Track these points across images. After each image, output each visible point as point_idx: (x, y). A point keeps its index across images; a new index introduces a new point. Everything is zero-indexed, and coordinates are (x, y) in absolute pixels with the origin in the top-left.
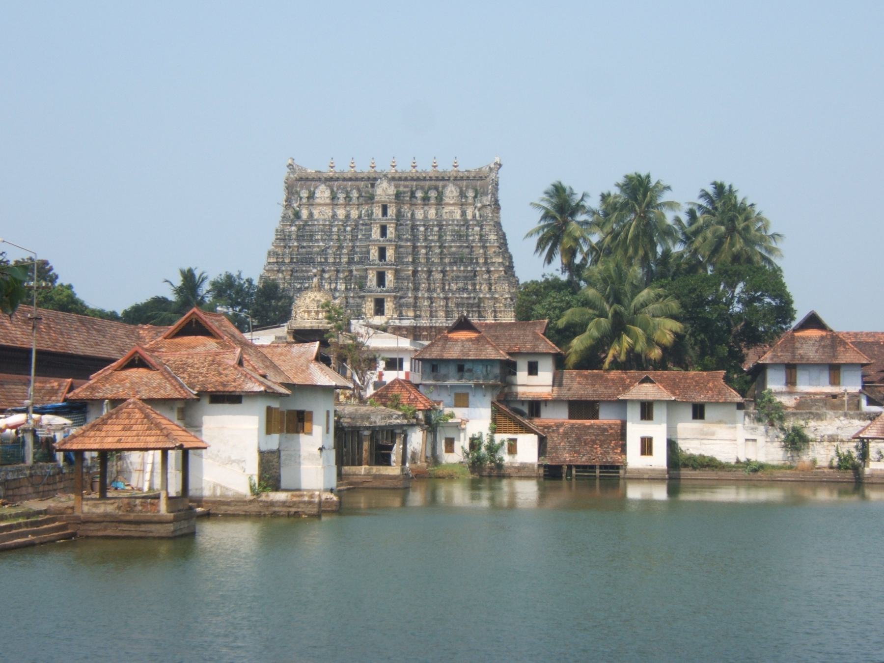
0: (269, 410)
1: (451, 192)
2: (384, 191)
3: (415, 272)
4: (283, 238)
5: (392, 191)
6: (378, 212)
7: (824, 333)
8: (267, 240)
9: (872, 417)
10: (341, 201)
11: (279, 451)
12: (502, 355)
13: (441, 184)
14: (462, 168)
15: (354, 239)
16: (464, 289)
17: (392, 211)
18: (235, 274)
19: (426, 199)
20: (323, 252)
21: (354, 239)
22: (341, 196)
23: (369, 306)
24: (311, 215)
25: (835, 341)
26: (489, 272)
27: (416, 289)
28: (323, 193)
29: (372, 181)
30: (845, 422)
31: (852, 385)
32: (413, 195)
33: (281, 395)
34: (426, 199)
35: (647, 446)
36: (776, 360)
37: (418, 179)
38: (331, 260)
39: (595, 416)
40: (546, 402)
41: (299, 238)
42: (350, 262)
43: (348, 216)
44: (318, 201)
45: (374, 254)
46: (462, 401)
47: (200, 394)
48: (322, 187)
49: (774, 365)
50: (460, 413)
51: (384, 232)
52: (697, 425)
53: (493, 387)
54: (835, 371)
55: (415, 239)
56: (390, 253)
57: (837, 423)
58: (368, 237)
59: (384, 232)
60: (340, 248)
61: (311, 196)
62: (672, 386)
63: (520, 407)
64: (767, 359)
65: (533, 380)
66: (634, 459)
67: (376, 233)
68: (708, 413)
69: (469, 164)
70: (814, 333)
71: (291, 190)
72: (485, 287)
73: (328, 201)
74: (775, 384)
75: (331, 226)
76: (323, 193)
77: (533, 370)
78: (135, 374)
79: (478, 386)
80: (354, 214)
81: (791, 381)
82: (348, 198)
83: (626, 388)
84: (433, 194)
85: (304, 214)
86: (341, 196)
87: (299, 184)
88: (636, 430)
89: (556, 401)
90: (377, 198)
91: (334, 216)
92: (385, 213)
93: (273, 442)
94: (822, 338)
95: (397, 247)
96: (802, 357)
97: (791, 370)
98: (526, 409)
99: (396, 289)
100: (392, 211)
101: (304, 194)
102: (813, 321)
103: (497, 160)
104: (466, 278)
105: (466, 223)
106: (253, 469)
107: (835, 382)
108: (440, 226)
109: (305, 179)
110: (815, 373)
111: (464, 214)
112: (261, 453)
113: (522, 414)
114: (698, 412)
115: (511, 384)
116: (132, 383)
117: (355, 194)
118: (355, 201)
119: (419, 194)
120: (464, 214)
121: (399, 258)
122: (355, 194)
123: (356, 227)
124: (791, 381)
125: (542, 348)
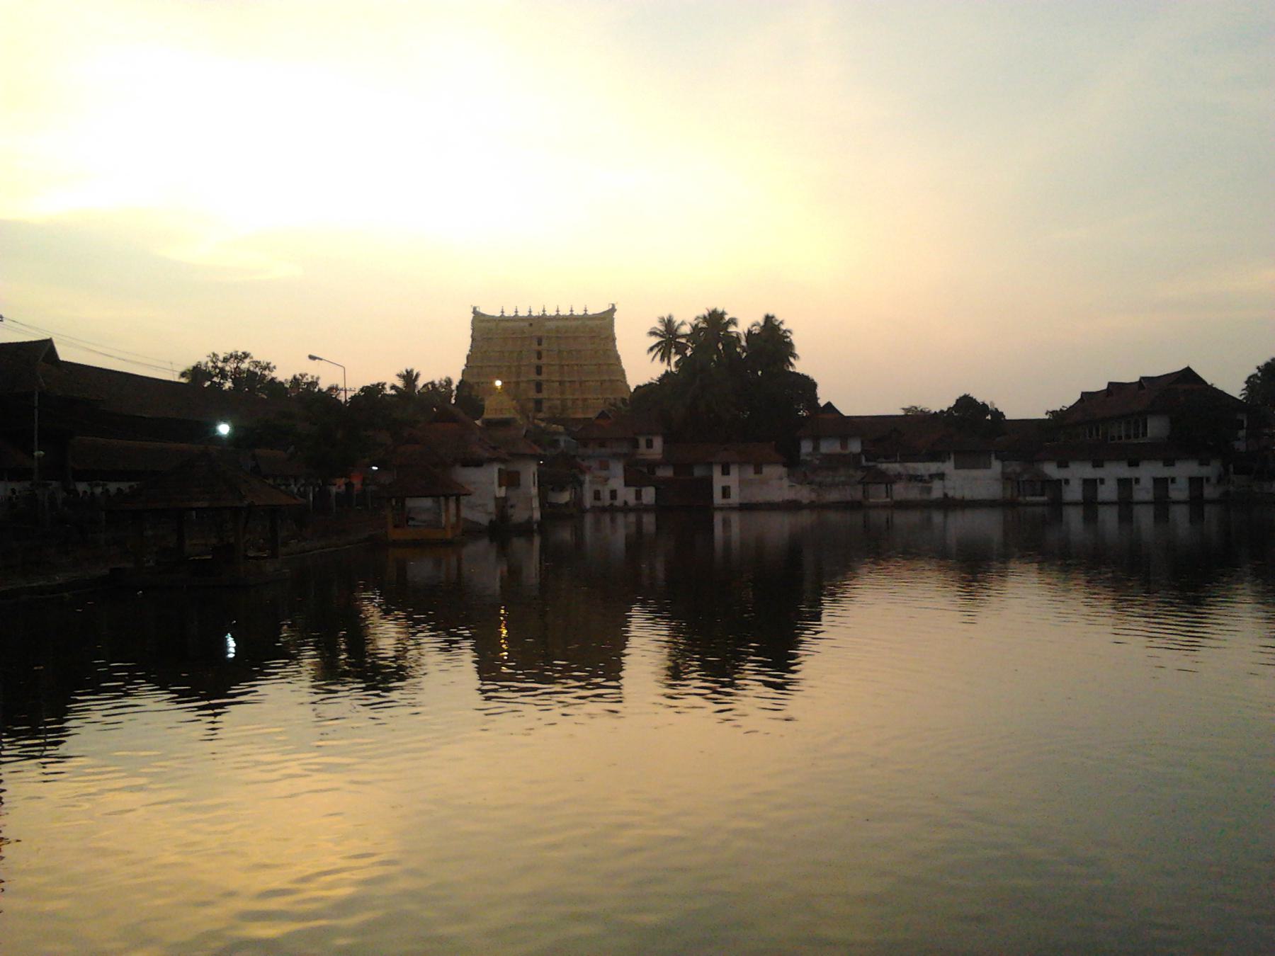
9: (868, 468)
14: (590, 313)
30: (851, 472)
35: (726, 492)
50: (604, 473)
52: (757, 476)
65: (651, 451)
66: (718, 499)
74: (806, 447)
77: (650, 444)
81: (816, 448)
88: (719, 481)
93: (501, 492)
97: (816, 440)
98: (645, 470)
106: (491, 507)
114: (758, 471)
124: (816, 448)
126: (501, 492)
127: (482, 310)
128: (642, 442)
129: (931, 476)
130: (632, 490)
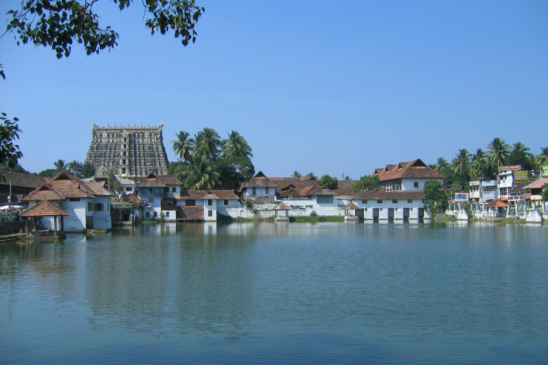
0: (89, 203)
1: (147, 134)
2: (125, 133)
3: (135, 160)
4: (92, 148)
5: (128, 133)
6: (123, 140)
8: (87, 150)
9: (278, 203)
10: (111, 137)
11: (92, 216)
12: (164, 186)
13: (143, 131)
14: (150, 126)
15: (115, 149)
16: (152, 165)
17: (128, 140)
18: (76, 160)
19: (138, 136)
21: (115, 149)
22: (111, 135)
23: (120, 170)
24: (101, 141)
25: (267, 180)
26: (159, 159)
27: (136, 165)
28: (105, 134)
29: (121, 130)
31: (272, 192)
32: (135, 135)
33: (93, 198)
34: (138, 136)
37: (136, 130)
39: (194, 204)
40: (178, 200)
41: (97, 149)
42: (114, 156)
43: (113, 141)
45: (122, 153)
46: (151, 200)
47: (66, 198)
49: (249, 188)
51: (125, 147)
53: (162, 196)
54: (267, 189)
55: (135, 149)
56: (127, 153)
57: (268, 205)
58: (120, 148)
59: (125, 147)
61: (101, 136)
62: (218, 195)
63: (169, 201)
64: (247, 186)
66: (206, 217)
67: (122, 147)
68: (230, 203)
69: (153, 125)
71: (95, 134)
72: (158, 164)
76: (105, 134)
77: (174, 190)
78: (44, 192)
79: (156, 196)
81: (254, 194)
82: (113, 136)
83: (204, 195)
84: (141, 135)
85: (99, 141)
86: (111, 135)
87: (97, 132)
89: (181, 200)
91: (109, 141)
92: (125, 140)
93: (91, 213)
94: (263, 179)
98: (172, 203)
101: (99, 134)
102: (261, 174)
103: (162, 123)
104: (152, 161)
105: (152, 144)
107: (267, 192)
108: (143, 145)
110: (261, 190)
111: (151, 141)
112: (86, 217)
113: (170, 204)
115: (167, 195)
116: (44, 195)
117: (115, 135)
119: (137, 135)
120: (151, 141)
122: (115, 135)
123: (116, 145)
124: (254, 194)
125: (177, 183)
126: (91, 213)
127: (97, 124)
128: (171, 189)
129: (306, 206)
130: (165, 212)
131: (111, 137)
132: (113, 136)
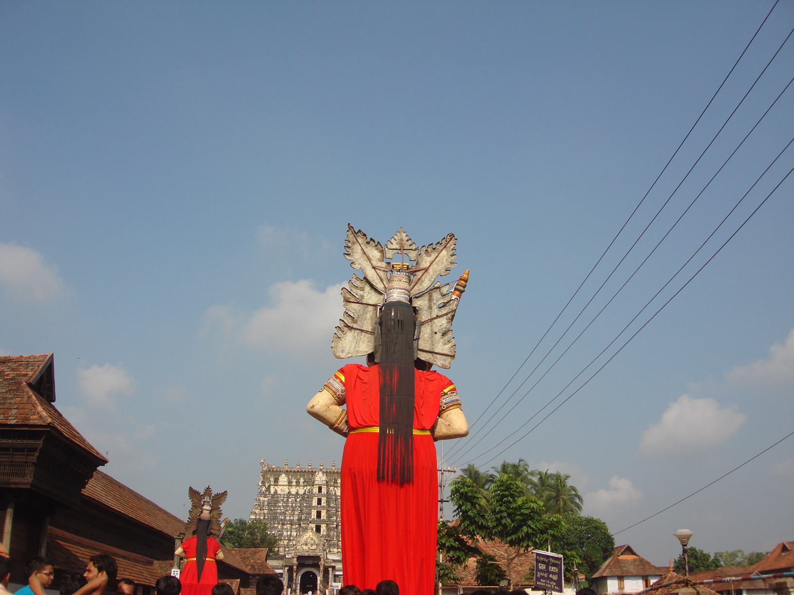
7: (634, 557)
10: (294, 483)
20: (284, 513)
22: (294, 481)
24: (276, 492)
36: (613, 574)
38: (288, 518)
43: (297, 493)
44: (280, 483)
48: (283, 475)
49: (612, 577)
58: (310, 507)
60: (293, 510)
61: (276, 480)
67: (315, 503)
70: (629, 557)
73: (286, 483)
75: (288, 498)
76: (283, 479)
80: (301, 492)
86: (294, 481)
90: (316, 482)
94: (635, 560)
95: (328, 511)
96: (627, 572)
99: (328, 535)
100: (324, 490)
102: (629, 550)
109: (271, 471)
117: (302, 480)
118: (301, 483)
121: (329, 516)
122: (302, 480)
131: (294, 483)
132: (298, 483)
